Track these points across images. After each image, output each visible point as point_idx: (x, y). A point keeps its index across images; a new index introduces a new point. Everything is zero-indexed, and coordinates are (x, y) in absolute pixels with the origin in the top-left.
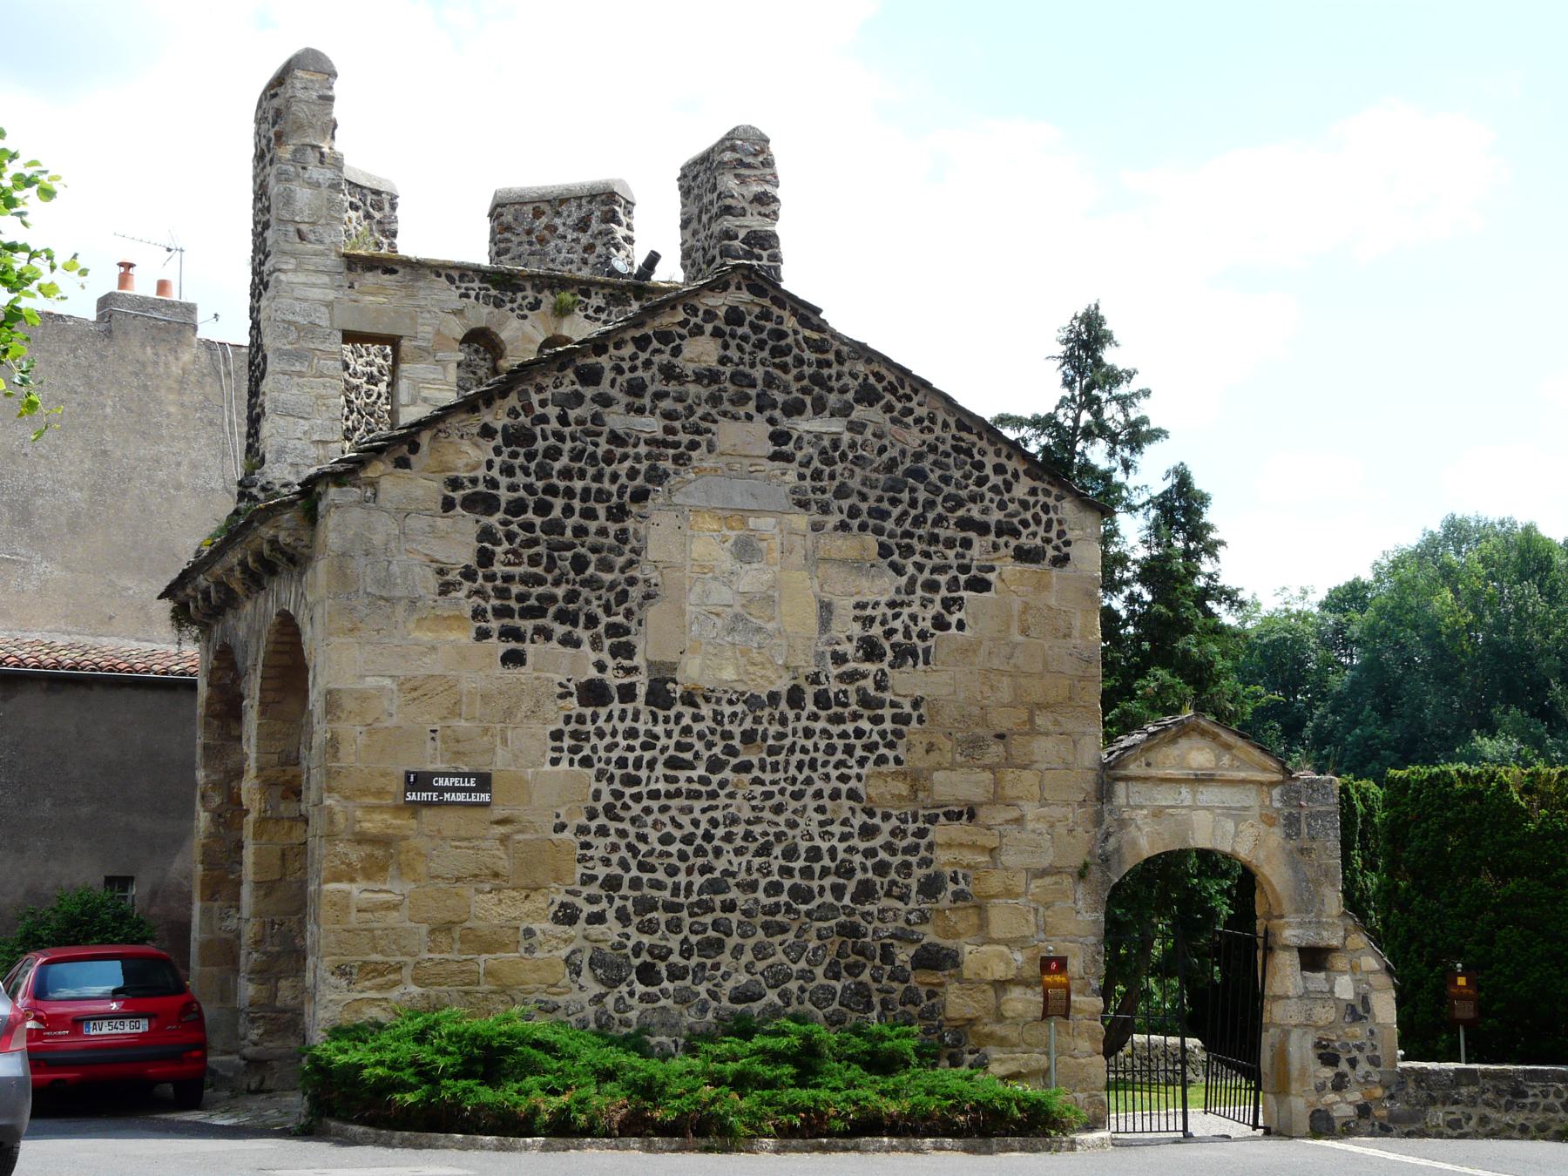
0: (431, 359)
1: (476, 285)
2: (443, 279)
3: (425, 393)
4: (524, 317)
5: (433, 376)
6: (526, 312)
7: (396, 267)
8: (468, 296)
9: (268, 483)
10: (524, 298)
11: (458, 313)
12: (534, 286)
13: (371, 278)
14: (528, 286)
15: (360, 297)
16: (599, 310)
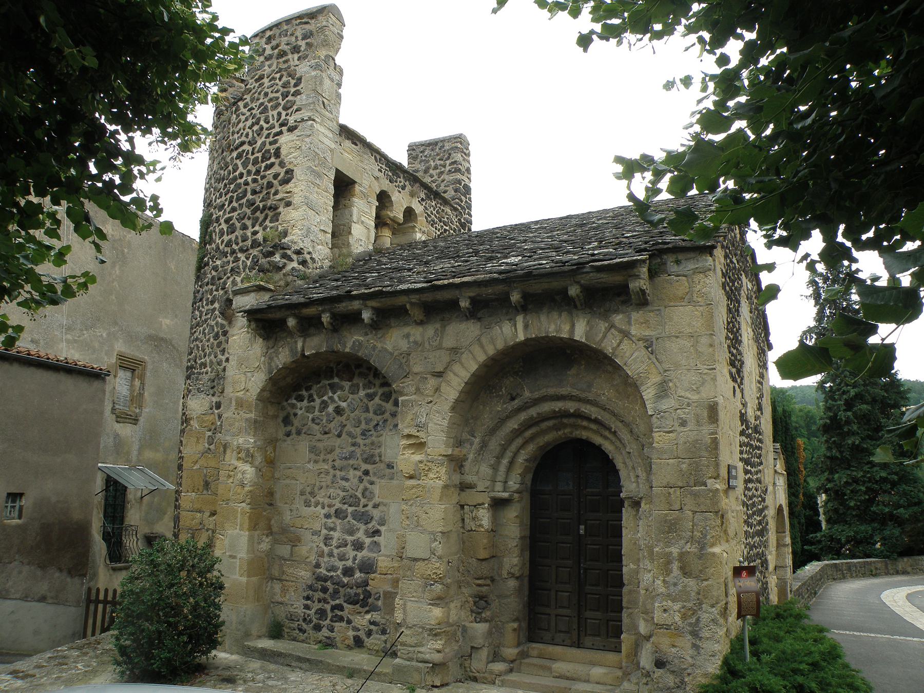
0: (365, 200)
1: (384, 166)
2: (373, 157)
3: (363, 218)
4: (400, 192)
5: (366, 210)
6: (400, 189)
7: (358, 143)
8: (381, 172)
9: (302, 249)
10: (400, 182)
11: (377, 178)
12: (404, 177)
13: (348, 144)
14: (402, 176)
15: (343, 152)
16: (422, 199)
